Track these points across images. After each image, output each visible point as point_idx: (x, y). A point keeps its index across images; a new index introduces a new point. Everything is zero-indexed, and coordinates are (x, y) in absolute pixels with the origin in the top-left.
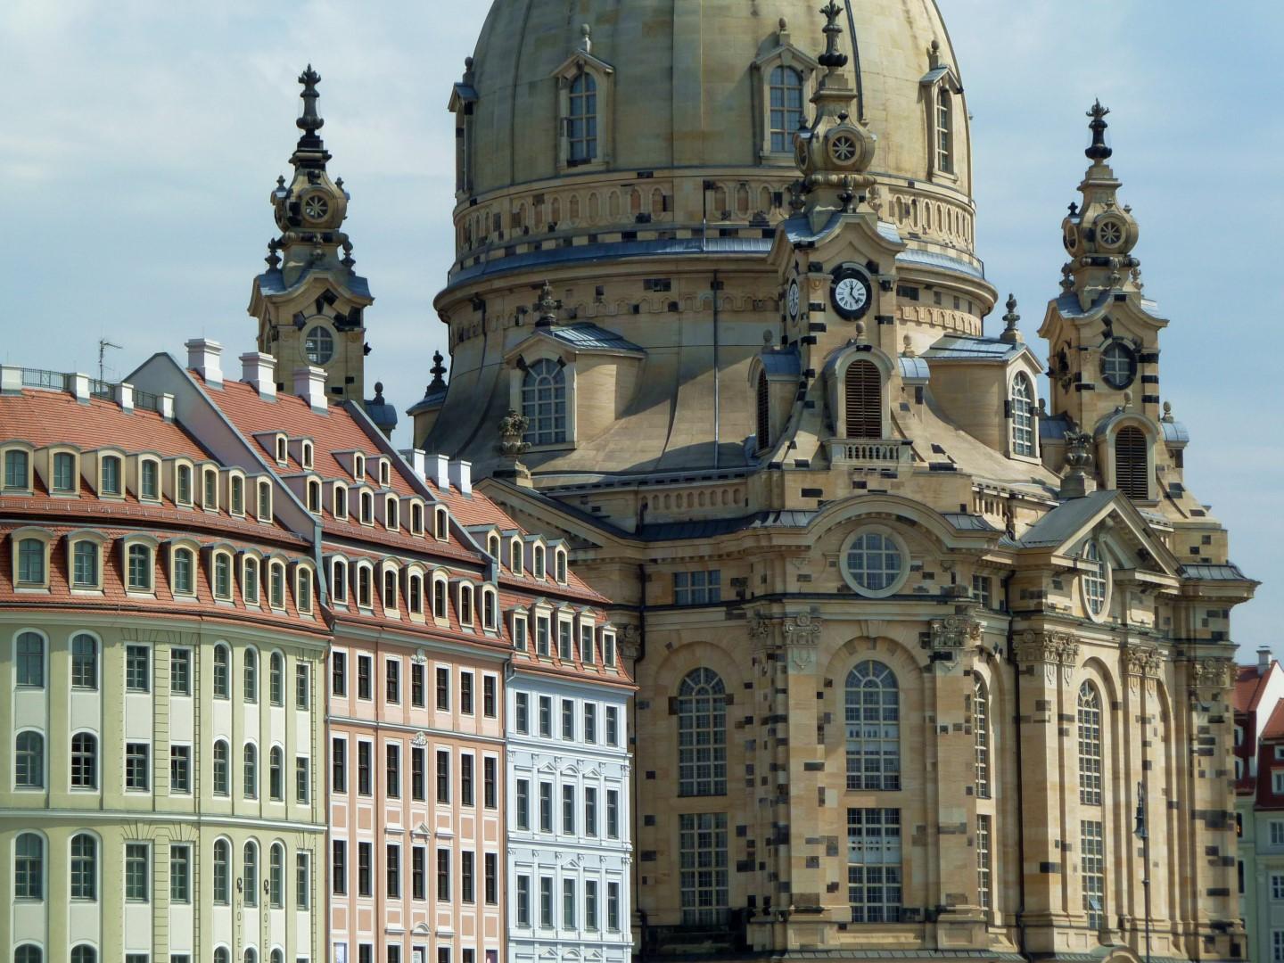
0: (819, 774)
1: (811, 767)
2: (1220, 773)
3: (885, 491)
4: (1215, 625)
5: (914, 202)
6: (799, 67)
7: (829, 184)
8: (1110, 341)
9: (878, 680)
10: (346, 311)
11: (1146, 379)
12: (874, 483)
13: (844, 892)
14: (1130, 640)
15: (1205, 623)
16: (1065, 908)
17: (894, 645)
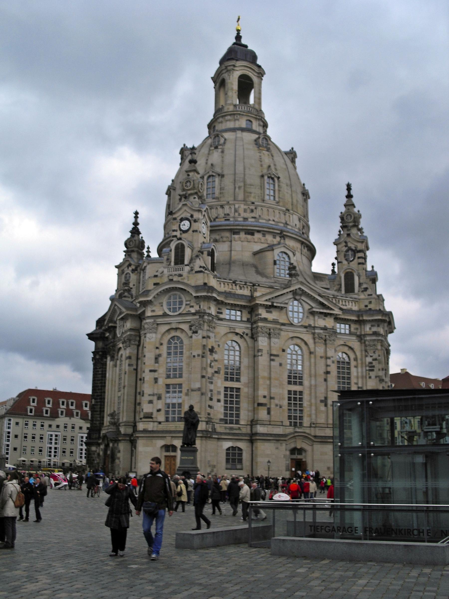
0: (156, 373)
1: (151, 371)
2: (376, 377)
3: (179, 281)
4: (375, 329)
5: (256, 208)
6: (214, 174)
7: (183, 195)
8: (347, 248)
9: (178, 342)
10: (133, 267)
11: (359, 258)
12: (175, 279)
13: (163, 412)
14: (317, 331)
15: (370, 329)
16: (270, 418)
17: (182, 330)
